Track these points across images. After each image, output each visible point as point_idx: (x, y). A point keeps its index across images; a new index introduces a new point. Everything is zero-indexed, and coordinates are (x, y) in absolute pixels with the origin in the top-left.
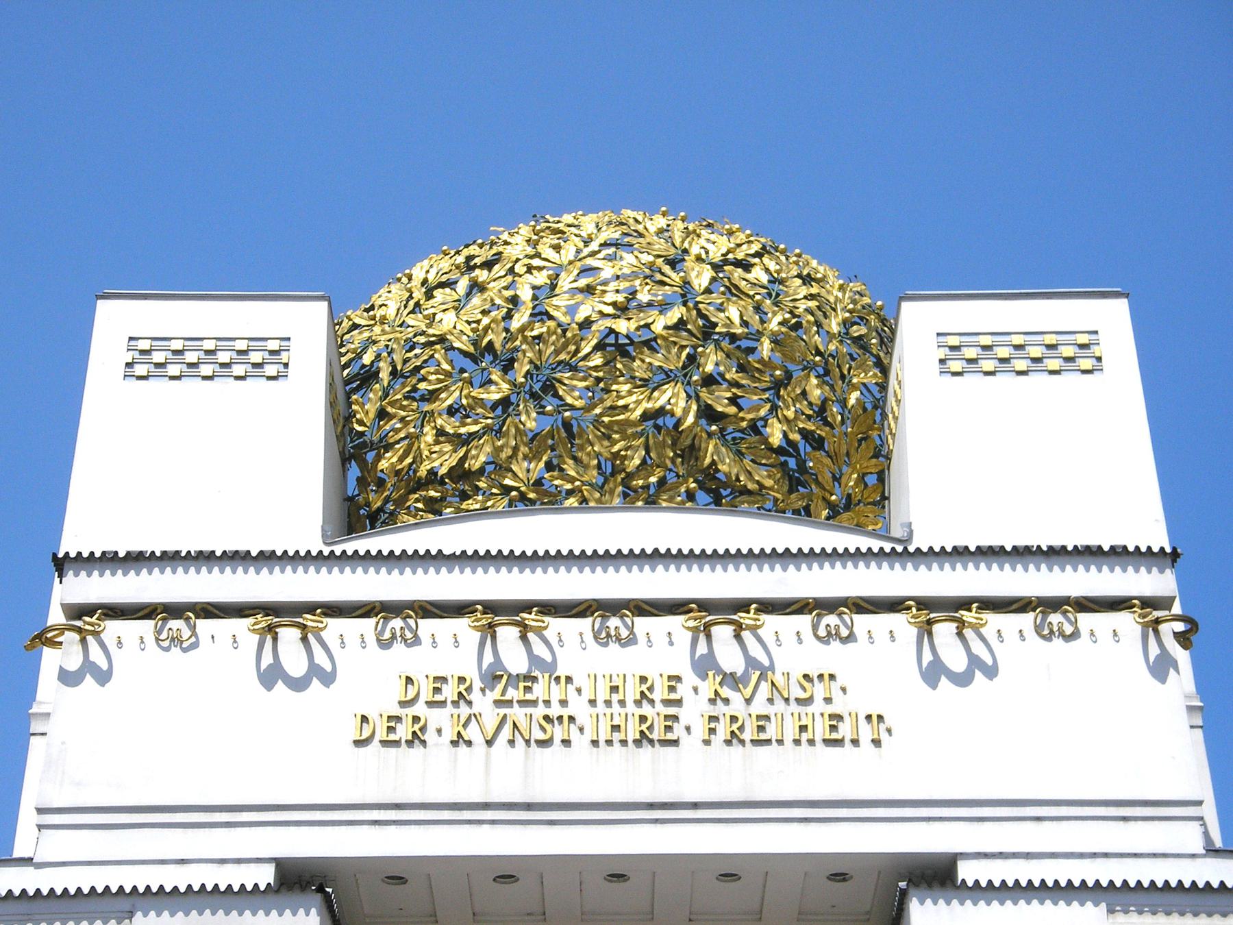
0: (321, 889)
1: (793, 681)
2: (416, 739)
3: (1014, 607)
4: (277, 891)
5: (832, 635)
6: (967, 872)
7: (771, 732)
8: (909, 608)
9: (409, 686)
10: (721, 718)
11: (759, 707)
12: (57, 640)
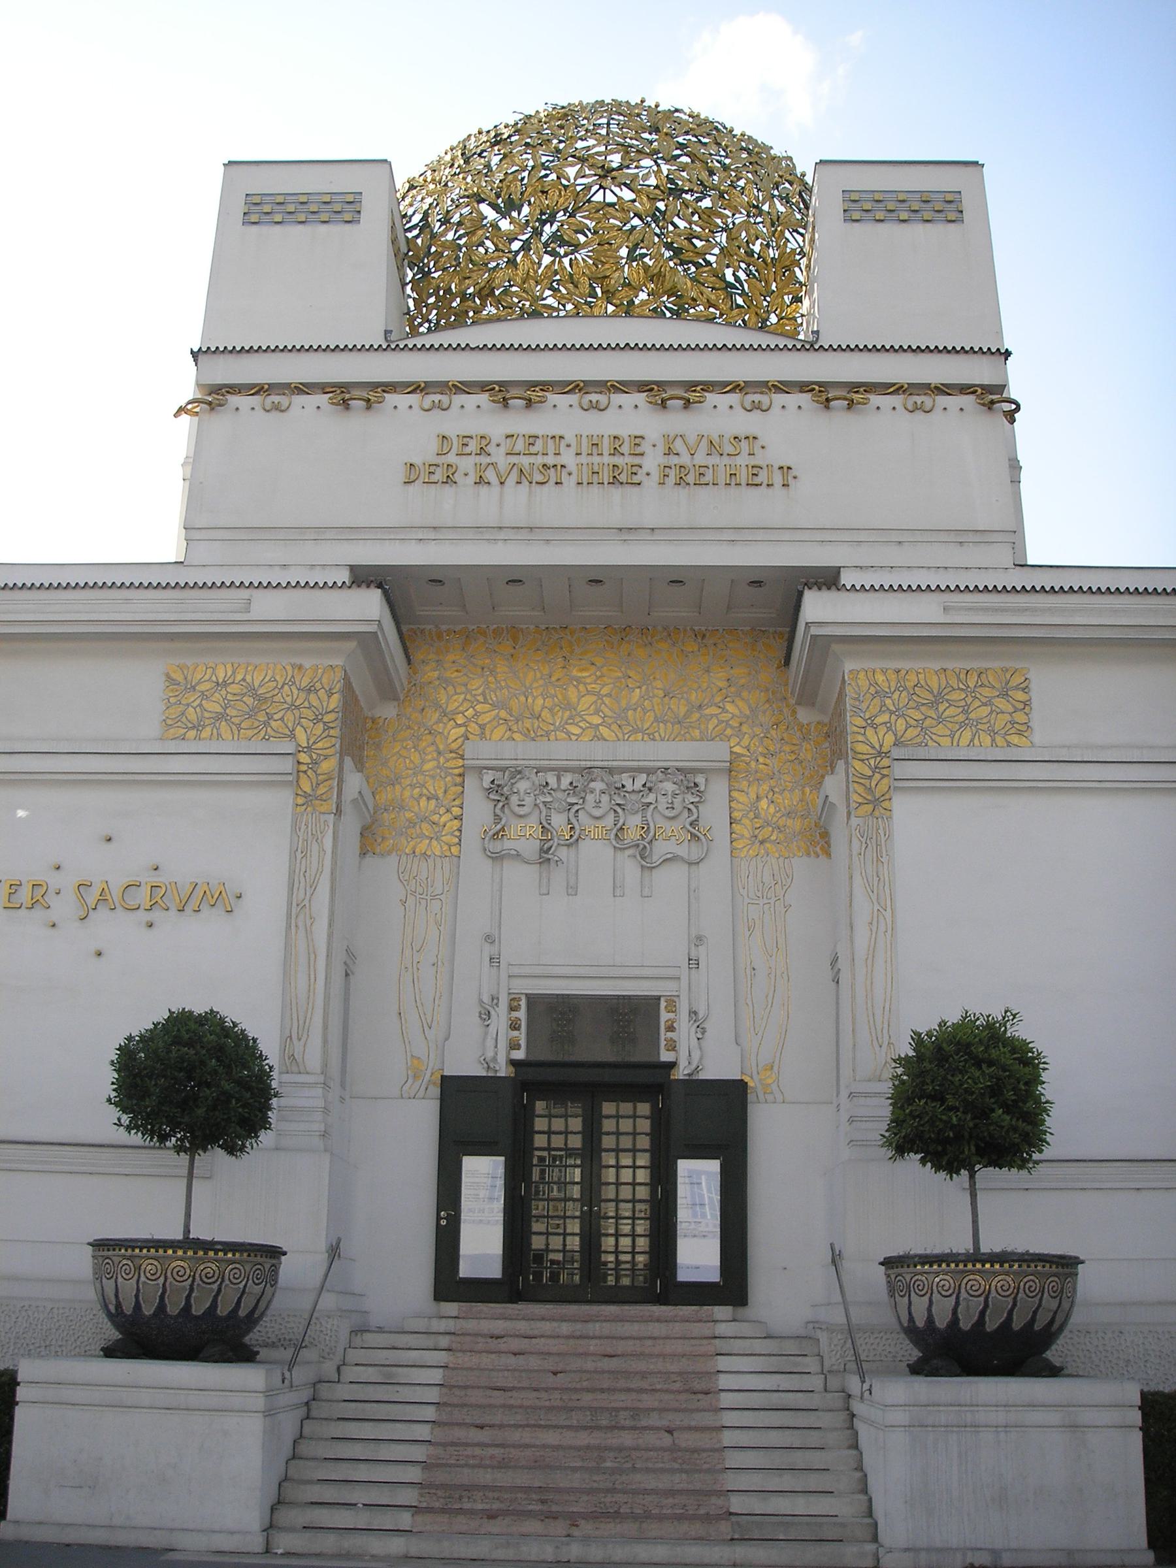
0: (380, 586)
1: (725, 440)
2: (449, 480)
4: (350, 587)
5: (757, 407)
7: (708, 478)
9: (445, 441)
10: (673, 467)
11: (700, 459)
12: (195, 410)
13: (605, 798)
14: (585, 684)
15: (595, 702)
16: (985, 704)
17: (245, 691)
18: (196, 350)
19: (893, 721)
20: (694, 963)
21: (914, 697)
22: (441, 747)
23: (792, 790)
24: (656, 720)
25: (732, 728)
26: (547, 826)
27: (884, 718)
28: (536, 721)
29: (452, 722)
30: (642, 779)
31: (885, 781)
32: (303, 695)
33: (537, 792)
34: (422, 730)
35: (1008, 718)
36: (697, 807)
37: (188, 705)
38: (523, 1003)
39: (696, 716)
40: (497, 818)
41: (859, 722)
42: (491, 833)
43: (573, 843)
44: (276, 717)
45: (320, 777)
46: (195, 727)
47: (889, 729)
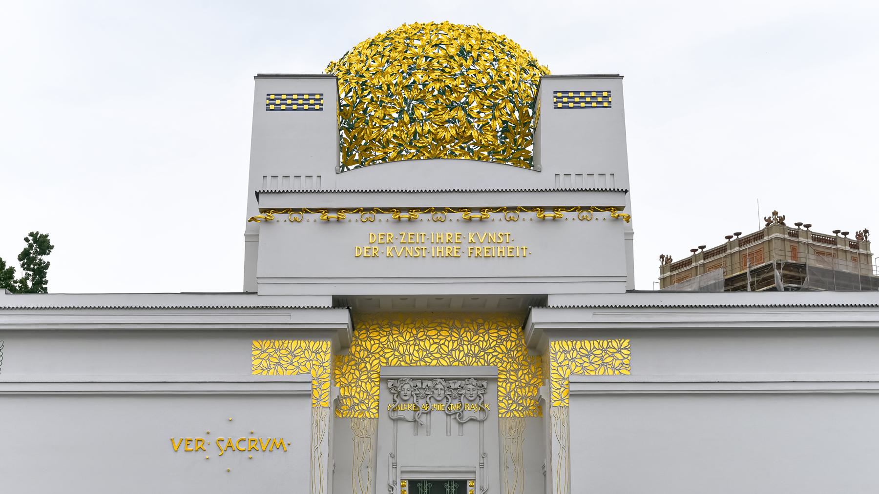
3: (572, 210)
5: (511, 220)
6: (551, 302)
8: (538, 210)
13: (443, 392)
14: (433, 339)
15: (438, 347)
16: (610, 356)
17: (288, 352)
18: (258, 191)
19: (570, 365)
20: (482, 466)
21: (579, 353)
22: (369, 369)
23: (524, 388)
24: (466, 355)
25: (499, 358)
26: (417, 404)
27: (566, 362)
28: (411, 356)
29: (374, 358)
30: (459, 383)
31: (566, 390)
32: (314, 354)
33: (412, 390)
34: (360, 360)
35: (621, 361)
36: (483, 395)
37: (263, 359)
38: (407, 484)
39: (482, 353)
40: (395, 401)
41: (555, 364)
42: (392, 408)
43: (428, 413)
44: (302, 364)
45: (323, 392)
46: (265, 369)
47: (568, 367)
